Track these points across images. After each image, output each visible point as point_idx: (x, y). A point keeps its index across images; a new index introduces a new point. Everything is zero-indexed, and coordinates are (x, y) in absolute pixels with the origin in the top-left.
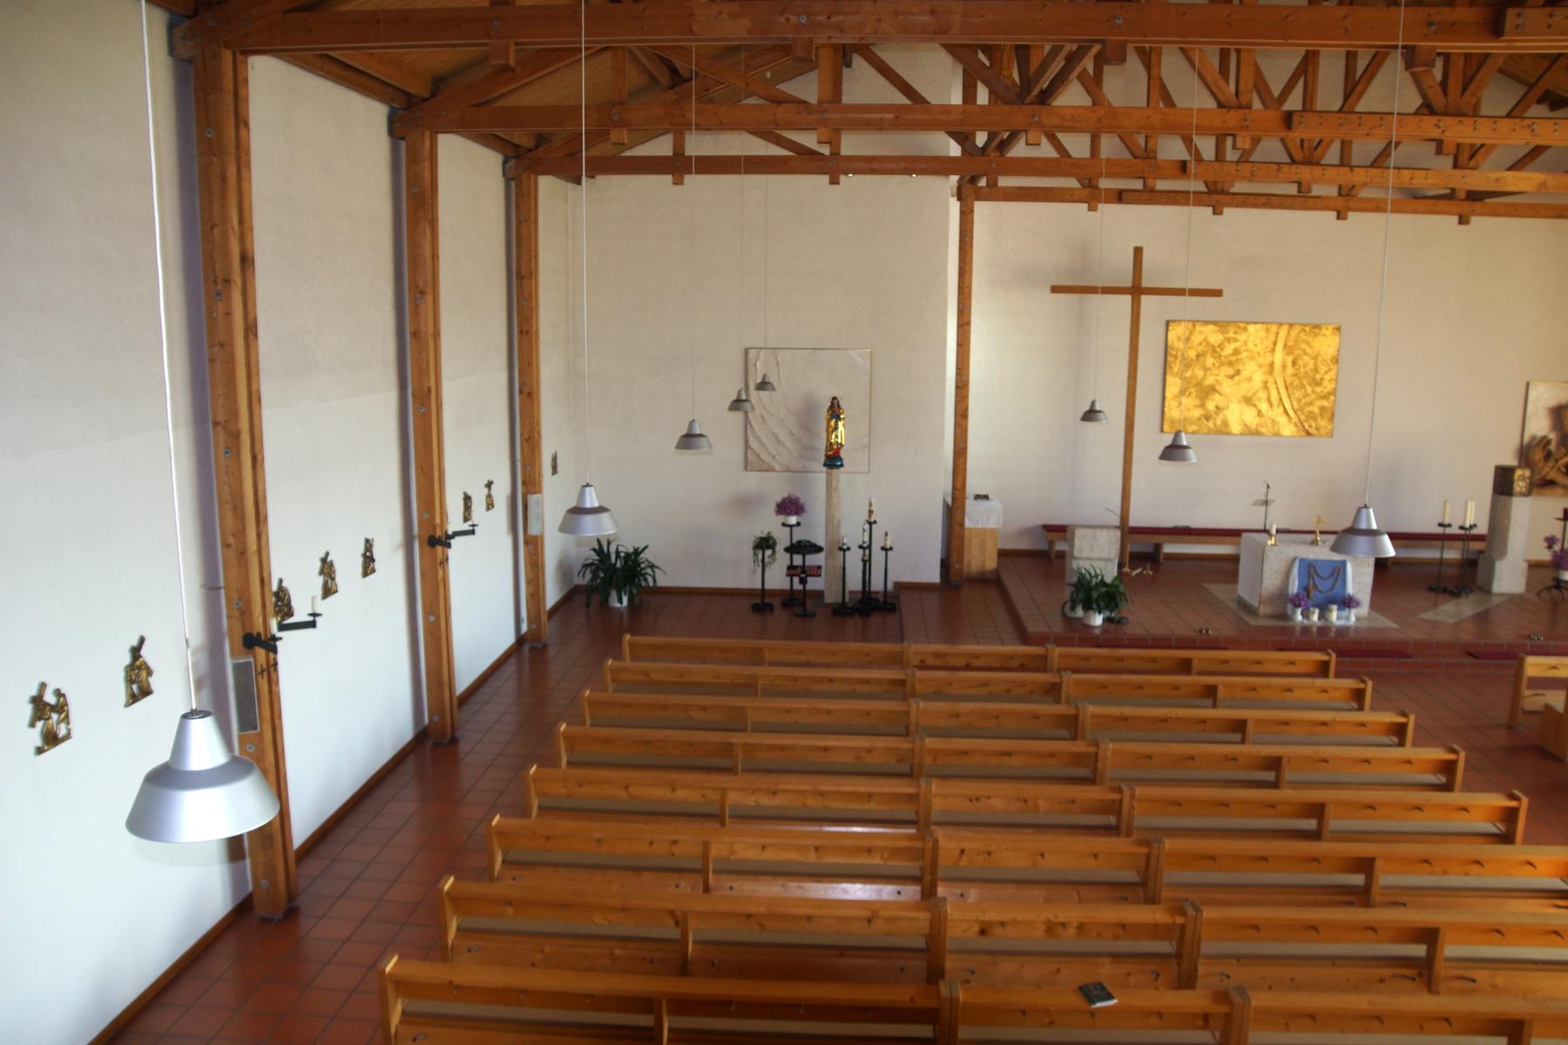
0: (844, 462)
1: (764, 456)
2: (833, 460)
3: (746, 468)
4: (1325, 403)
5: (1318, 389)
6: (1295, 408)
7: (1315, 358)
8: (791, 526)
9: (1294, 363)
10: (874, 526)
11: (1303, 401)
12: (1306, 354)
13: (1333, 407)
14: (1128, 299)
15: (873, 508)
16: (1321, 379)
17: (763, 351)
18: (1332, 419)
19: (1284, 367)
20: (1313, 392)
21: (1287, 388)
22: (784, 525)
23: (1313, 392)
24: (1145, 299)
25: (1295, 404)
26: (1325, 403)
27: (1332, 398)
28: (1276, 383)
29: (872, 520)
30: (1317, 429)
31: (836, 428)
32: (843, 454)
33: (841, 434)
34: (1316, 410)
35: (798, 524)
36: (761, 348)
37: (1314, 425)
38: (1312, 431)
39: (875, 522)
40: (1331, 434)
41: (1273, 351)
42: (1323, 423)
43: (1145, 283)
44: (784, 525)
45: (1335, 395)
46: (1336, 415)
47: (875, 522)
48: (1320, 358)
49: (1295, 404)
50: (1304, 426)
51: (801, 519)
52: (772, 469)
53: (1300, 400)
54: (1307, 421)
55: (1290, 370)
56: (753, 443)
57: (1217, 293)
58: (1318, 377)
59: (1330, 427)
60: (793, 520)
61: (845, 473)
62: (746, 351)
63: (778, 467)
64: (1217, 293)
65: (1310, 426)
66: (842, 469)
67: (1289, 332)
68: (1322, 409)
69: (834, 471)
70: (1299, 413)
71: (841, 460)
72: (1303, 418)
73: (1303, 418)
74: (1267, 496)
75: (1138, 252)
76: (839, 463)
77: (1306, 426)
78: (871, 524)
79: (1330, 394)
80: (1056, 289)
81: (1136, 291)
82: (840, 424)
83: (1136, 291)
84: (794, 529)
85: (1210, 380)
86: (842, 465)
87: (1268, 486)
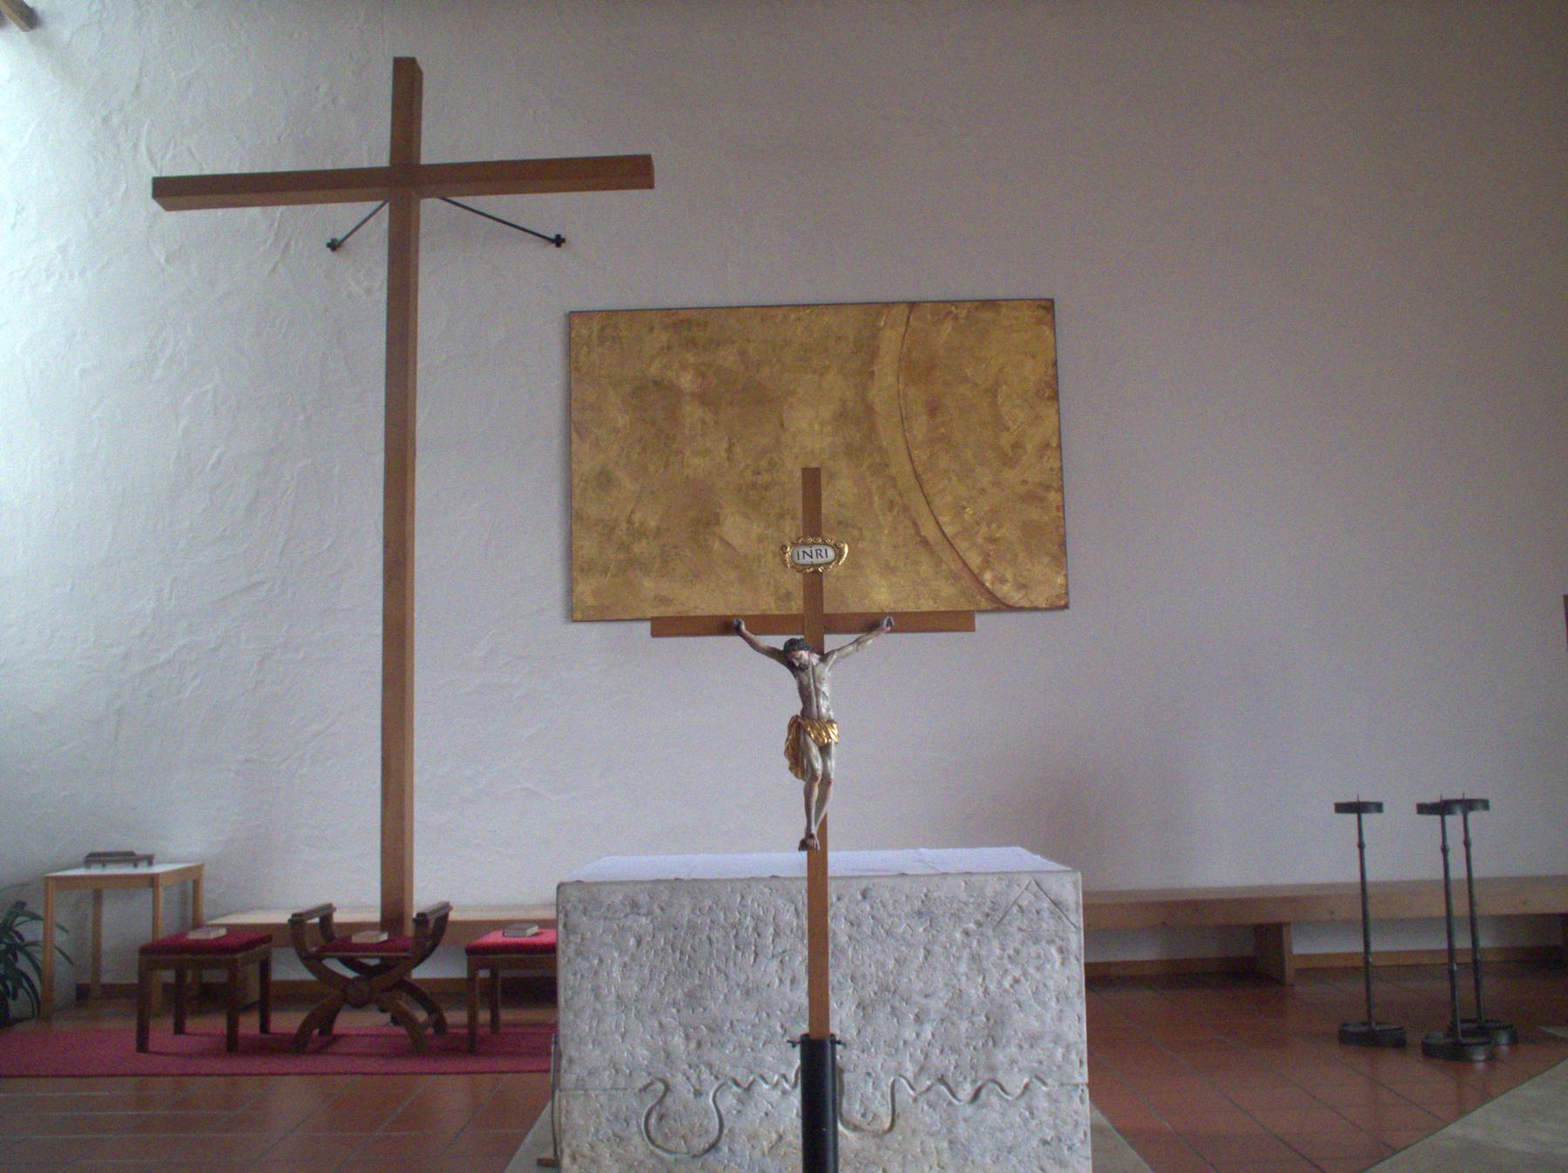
4: (1034, 513)
5: (1008, 475)
6: (949, 530)
7: (993, 391)
9: (933, 409)
13: (1060, 524)
16: (1017, 446)
20: (997, 484)
23: (997, 484)
27: (1053, 496)
34: (1008, 532)
37: (1009, 576)
38: (1007, 591)
45: (1061, 489)
53: (959, 511)
54: (987, 563)
55: (920, 428)
58: (1006, 440)
59: (1060, 580)
77: (987, 577)
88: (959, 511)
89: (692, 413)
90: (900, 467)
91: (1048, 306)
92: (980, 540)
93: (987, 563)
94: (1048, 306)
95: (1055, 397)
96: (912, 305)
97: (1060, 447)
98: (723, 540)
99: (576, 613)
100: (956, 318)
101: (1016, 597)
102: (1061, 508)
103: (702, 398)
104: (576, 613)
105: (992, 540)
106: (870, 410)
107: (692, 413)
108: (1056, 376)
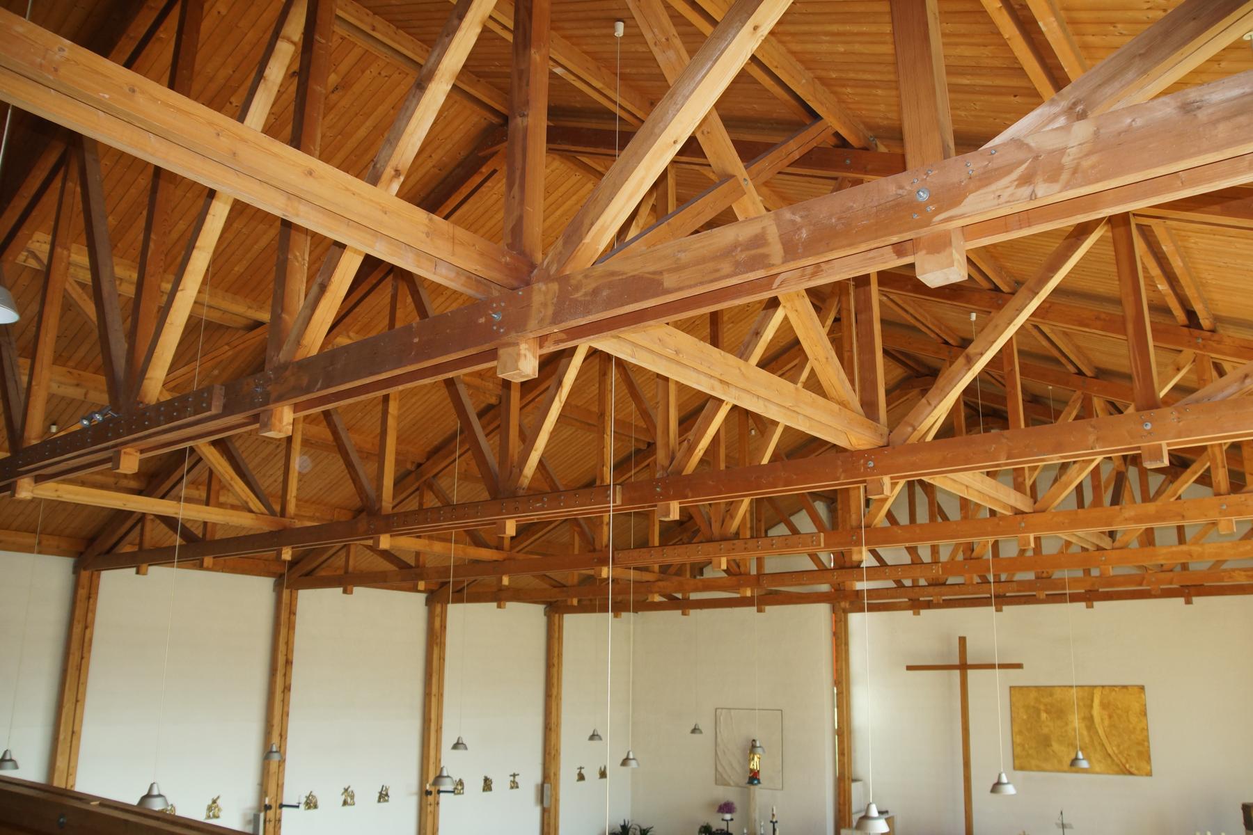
0: (761, 781)
1: (725, 776)
2: (754, 778)
3: (716, 784)
4: (1141, 748)
5: (1133, 736)
6: (1116, 752)
7: (1128, 712)
8: (727, 821)
9: (1110, 717)
10: (776, 825)
11: (1121, 747)
12: (1118, 709)
14: (957, 673)
15: (774, 812)
17: (724, 710)
18: (1149, 760)
19: (1102, 720)
21: (1107, 737)
22: (723, 820)
24: (970, 672)
25: (1114, 748)
26: (1141, 748)
28: (1097, 732)
29: (774, 820)
30: (1138, 769)
31: (753, 759)
32: (761, 776)
33: (755, 764)
34: (1134, 753)
35: (732, 820)
36: (722, 709)
37: (1134, 765)
38: (1133, 770)
39: (776, 822)
40: (1150, 774)
41: (1091, 707)
42: (1143, 764)
43: (969, 662)
44: (723, 820)
45: (1148, 742)
46: (1152, 758)
47: (776, 822)
48: (1130, 712)
49: (1114, 748)
50: (1126, 768)
51: (734, 816)
52: (728, 784)
56: (720, 768)
57: (1019, 666)
58: (1131, 726)
59: (1149, 768)
60: (728, 816)
61: (761, 788)
62: (716, 709)
63: (732, 783)
64: (1019, 666)
65: (1131, 767)
66: (760, 785)
67: (1102, 693)
68: (1140, 754)
69: (752, 787)
70: (1120, 756)
71: (759, 780)
72: (1124, 761)
73: (1124, 761)
74: (1062, 821)
75: (962, 640)
76: (756, 782)
77: (1127, 766)
78: (774, 823)
79: (1144, 740)
80: (909, 668)
81: (963, 667)
82: (756, 759)
83: (963, 667)
84: (730, 822)
85: (1045, 731)
86: (759, 783)
87: (1062, 813)
88: (1118, 746)
89: (1044, 716)
90: (1101, 732)
91: (1142, 688)
92: (1125, 755)
93: (1127, 762)
94: (1142, 688)
95: (1145, 715)
96: (1103, 687)
97: (1147, 729)
98: (1053, 751)
99: (1015, 768)
100: (1116, 691)
101: (1136, 772)
102: (1149, 747)
103: (1047, 711)
104: (1015, 768)
105: (1129, 755)
106: (1092, 717)
107: (1044, 716)
108: (1146, 709)
